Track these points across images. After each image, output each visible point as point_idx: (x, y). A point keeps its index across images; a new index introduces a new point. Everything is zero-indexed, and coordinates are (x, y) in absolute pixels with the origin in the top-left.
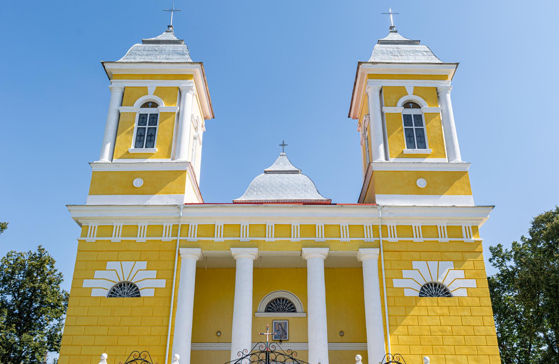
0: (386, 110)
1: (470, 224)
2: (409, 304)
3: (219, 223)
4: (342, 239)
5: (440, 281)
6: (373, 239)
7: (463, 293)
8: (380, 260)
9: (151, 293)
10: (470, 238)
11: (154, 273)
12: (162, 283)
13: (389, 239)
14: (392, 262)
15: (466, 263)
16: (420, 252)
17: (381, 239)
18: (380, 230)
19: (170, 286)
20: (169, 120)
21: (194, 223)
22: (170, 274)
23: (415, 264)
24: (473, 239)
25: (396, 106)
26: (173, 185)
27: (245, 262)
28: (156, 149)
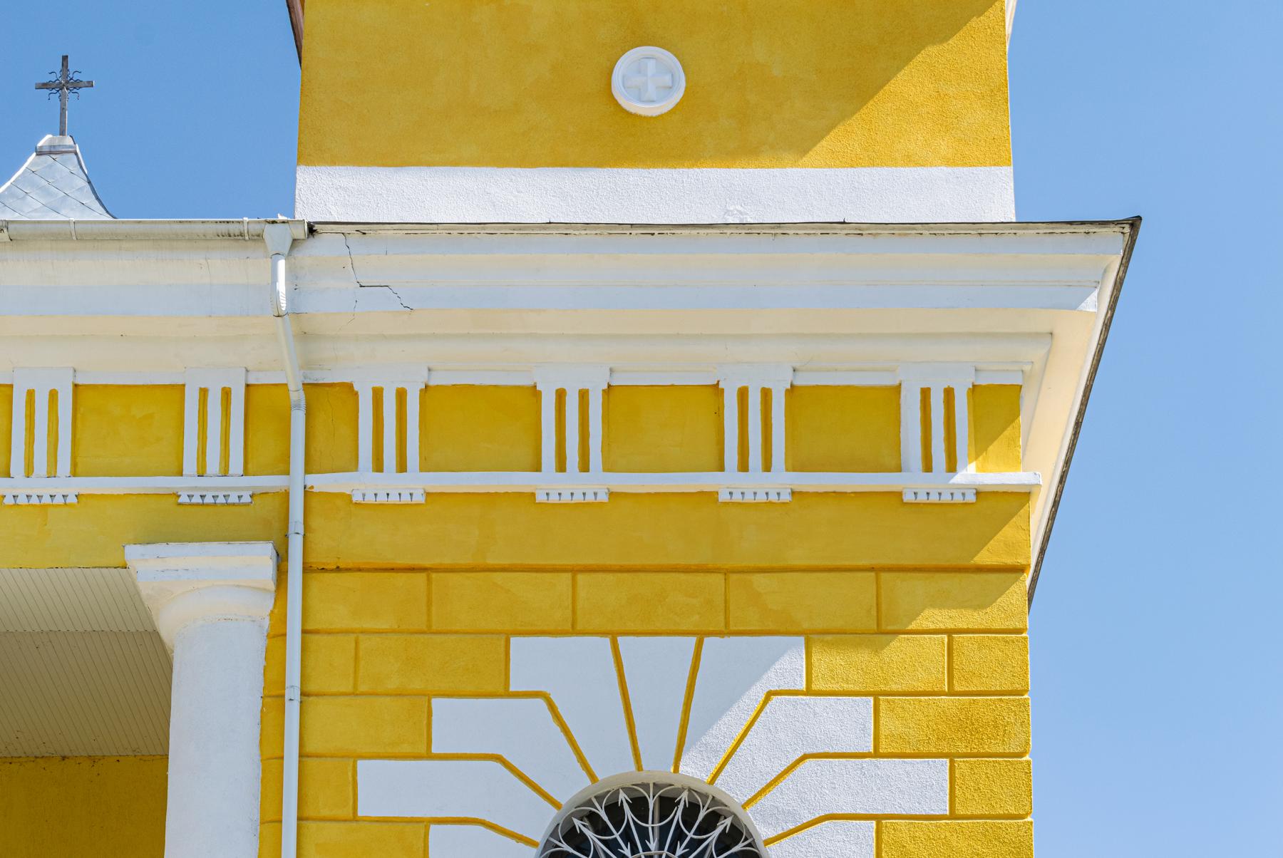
1: (956, 367)
5: (694, 770)
6: (240, 485)
8: (277, 635)
10: (952, 467)
13: (362, 484)
14: (367, 643)
15: (898, 648)
16: (575, 571)
18: (298, 419)
23: (532, 659)
24: (971, 474)
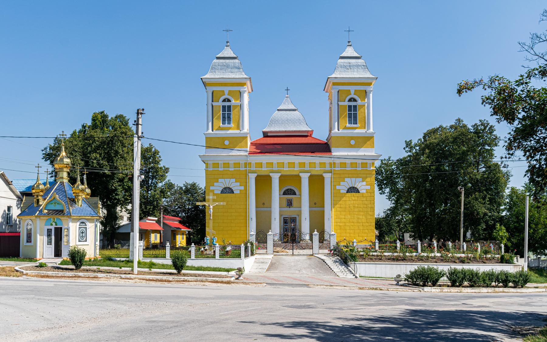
2: (342, 196)
3: (264, 162)
4: (316, 169)
5: (355, 186)
6: (329, 169)
7: (364, 191)
9: (238, 192)
11: (238, 184)
12: (242, 188)
13: (336, 169)
17: (333, 169)
19: (246, 189)
20: (237, 109)
21: (253, 162)
22: (246, 184)
23: (346, 179)
26: (243, 144)
27: (275, 178)
28: (232, 125)
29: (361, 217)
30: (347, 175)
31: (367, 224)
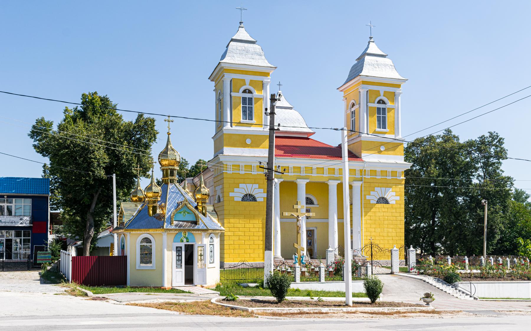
0: (370, 105)
5: (385, 197)
6: (360, 176)
7: (394, 202)
8: (361, 186)
13: (366, 177)
17: (364, 176)
23: (376, 189)
25: (374, 103)
28: (254, 121)
29: (390, 230)
30: (377, 185)
31: (397, 238)
